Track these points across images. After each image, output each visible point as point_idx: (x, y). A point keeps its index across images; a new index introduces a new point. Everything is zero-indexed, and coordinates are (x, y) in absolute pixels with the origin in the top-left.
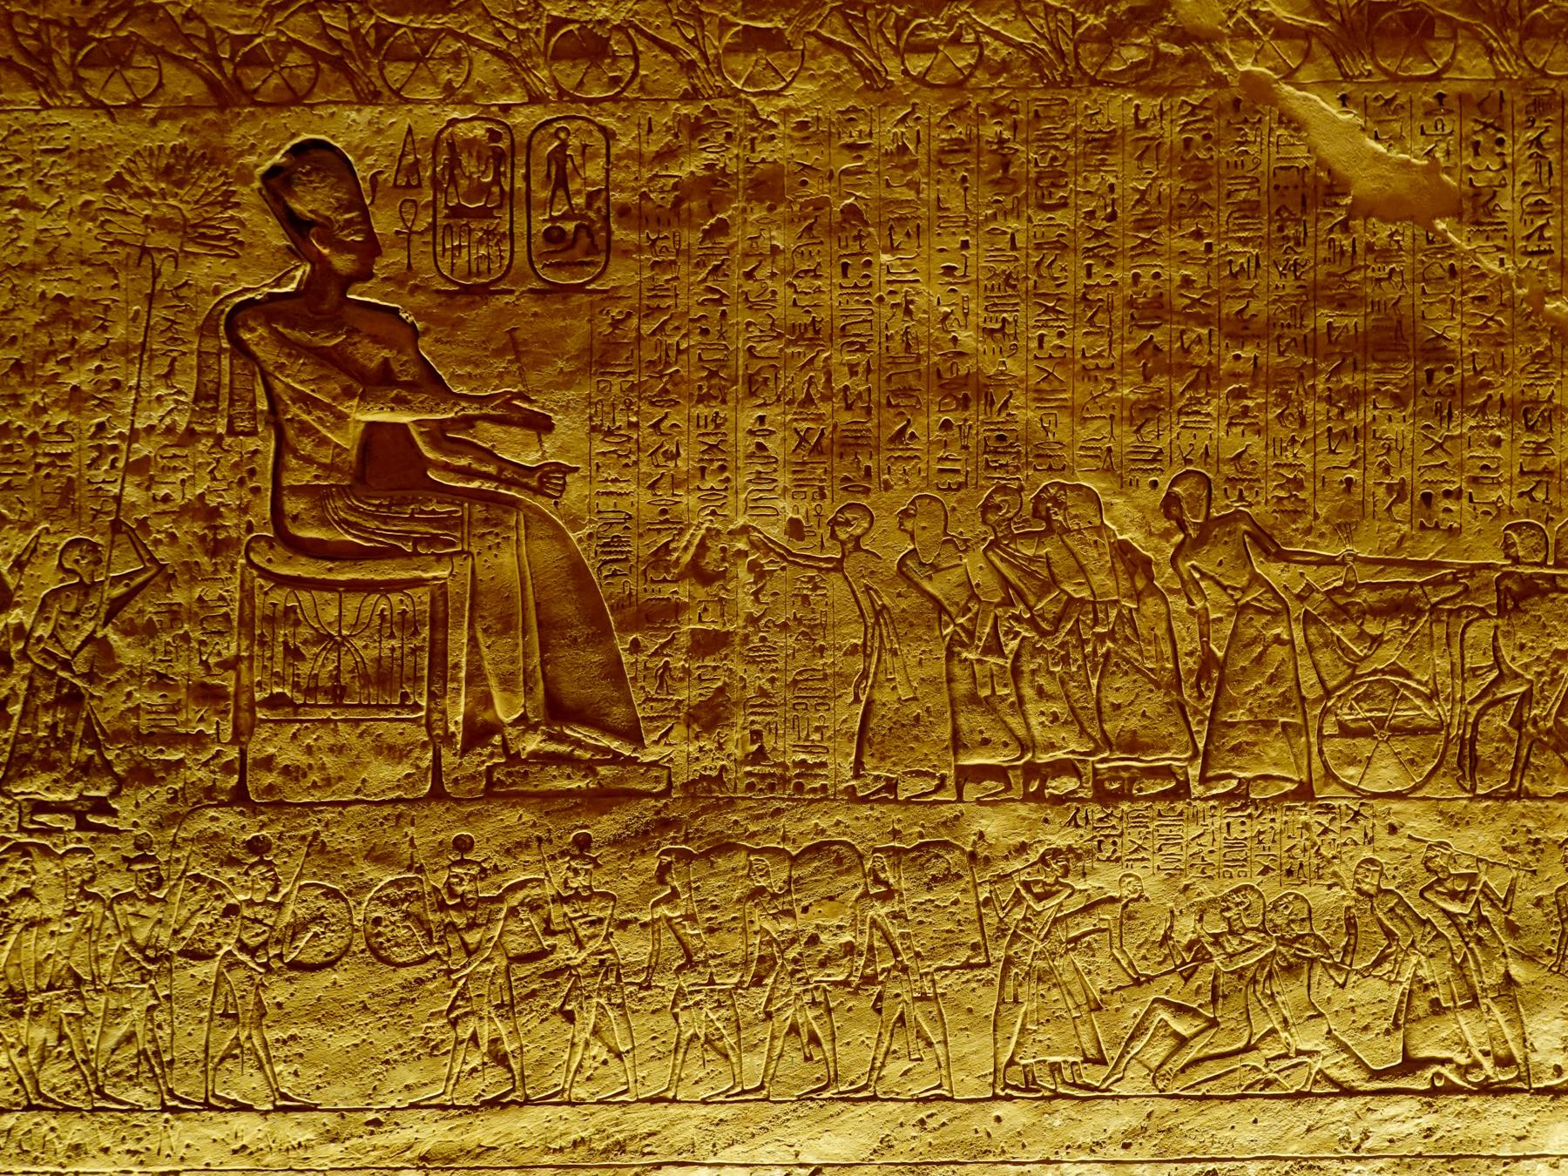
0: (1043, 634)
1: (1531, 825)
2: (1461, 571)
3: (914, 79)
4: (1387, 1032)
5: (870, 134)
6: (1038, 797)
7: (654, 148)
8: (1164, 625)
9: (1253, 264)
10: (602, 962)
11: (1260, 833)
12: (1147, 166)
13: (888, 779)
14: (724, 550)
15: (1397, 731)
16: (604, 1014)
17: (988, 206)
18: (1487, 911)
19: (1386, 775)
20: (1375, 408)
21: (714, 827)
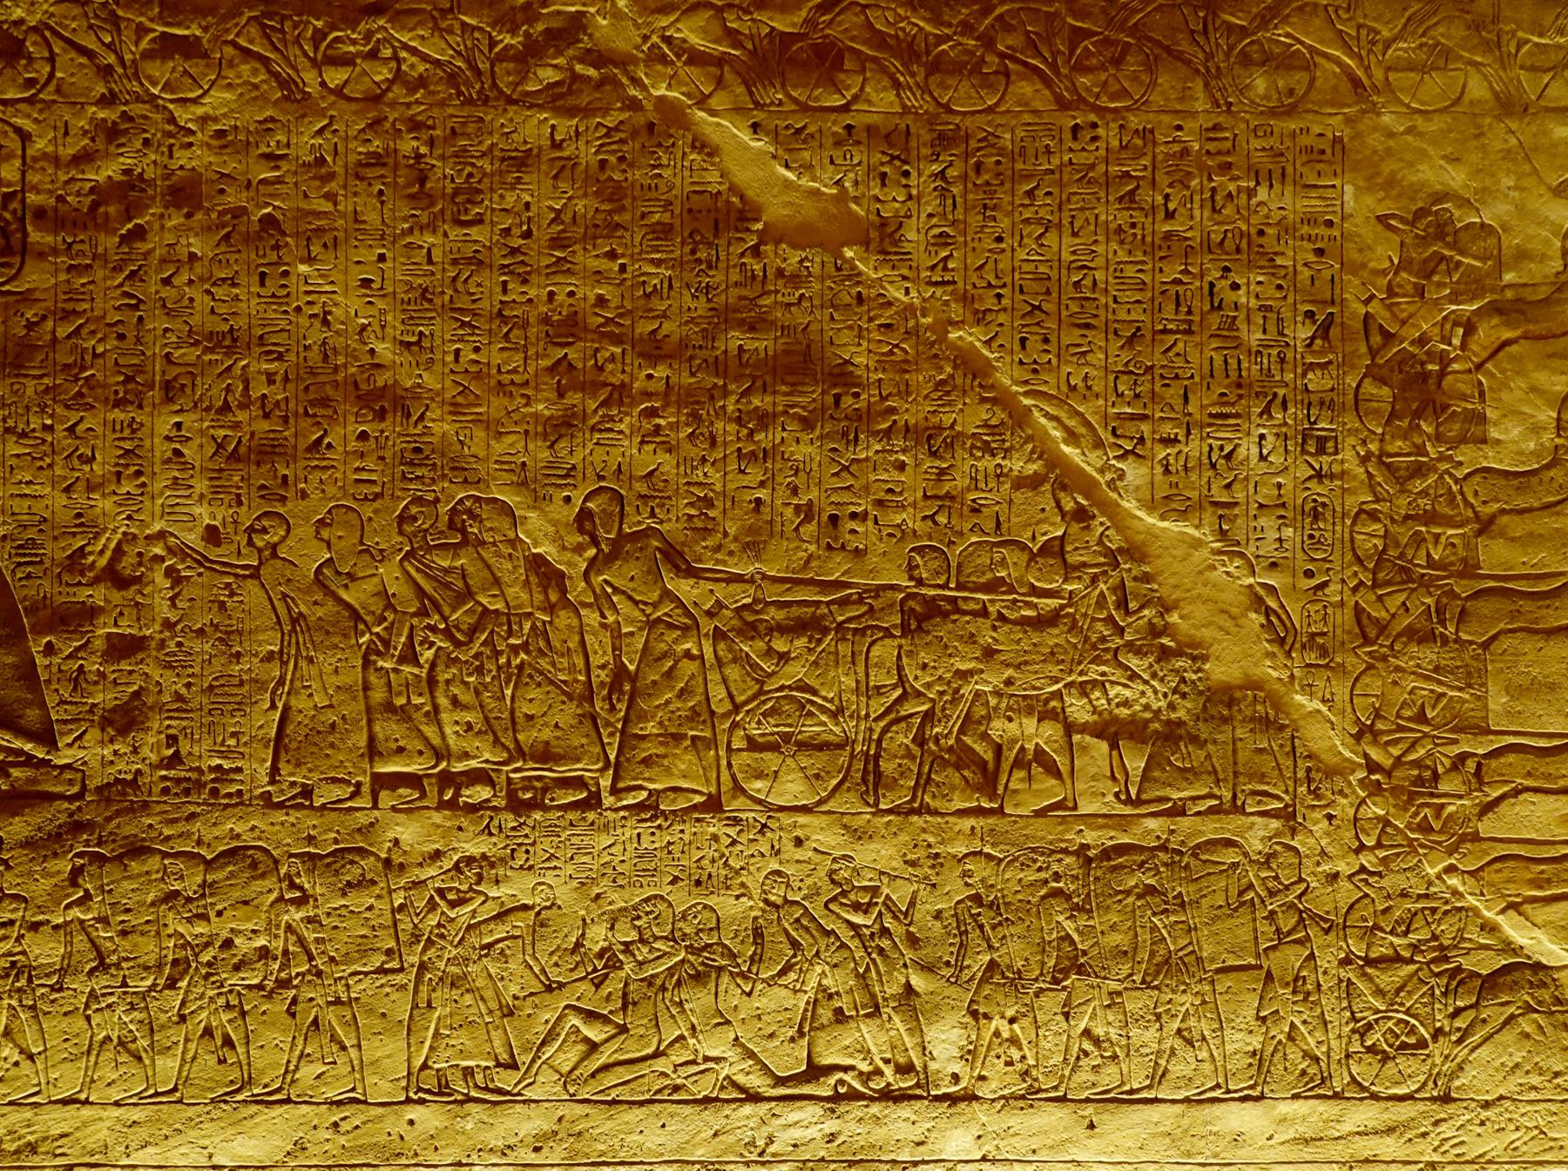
0: (458, 644)
1: (931, 839)
2: (866, 591)
3: (331, 91)
4: (792, 1040)
5: (288, 145)
6: (452, 805)
7: (71, 151)
8: (577, 638)
9: (666, 285)
10: (13, 964)
11: (669, 843)
12: (563, 185)
13: (304, 785)
14: (140, 554)
15: (803, 746)
16: (16, 1016)
17: (405, 220)
18: (888, 922)
19: (792, 789)
20: (784, 429)
21: (128, 830)
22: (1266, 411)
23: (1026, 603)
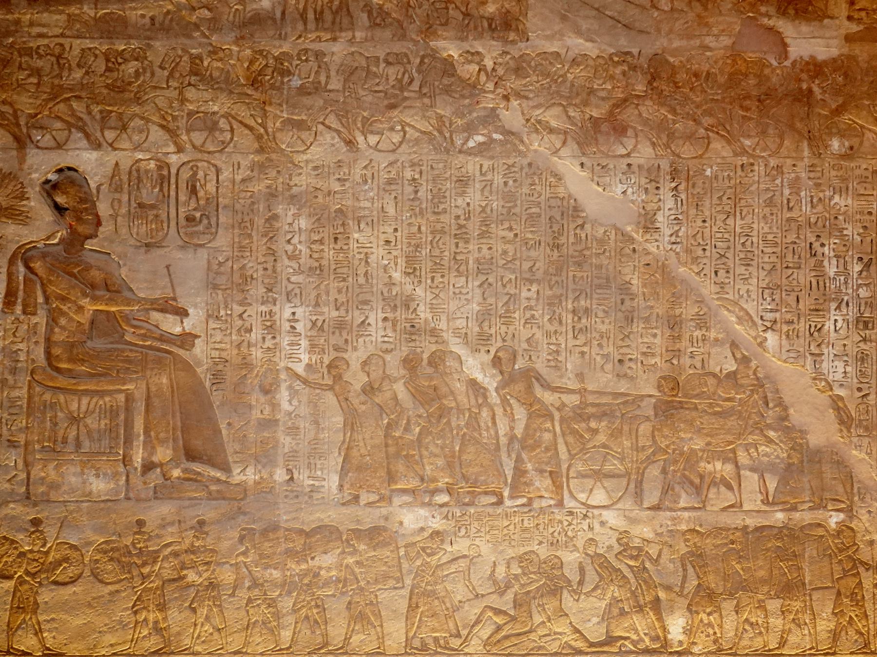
1: (669, 523)
4: (598, 623)
5: (349, 174)
6: (429, 504)
7: (240, 177)
16: (211, 610)
18: (648, 565)
22: (838, 308)
23: (718, 405)
